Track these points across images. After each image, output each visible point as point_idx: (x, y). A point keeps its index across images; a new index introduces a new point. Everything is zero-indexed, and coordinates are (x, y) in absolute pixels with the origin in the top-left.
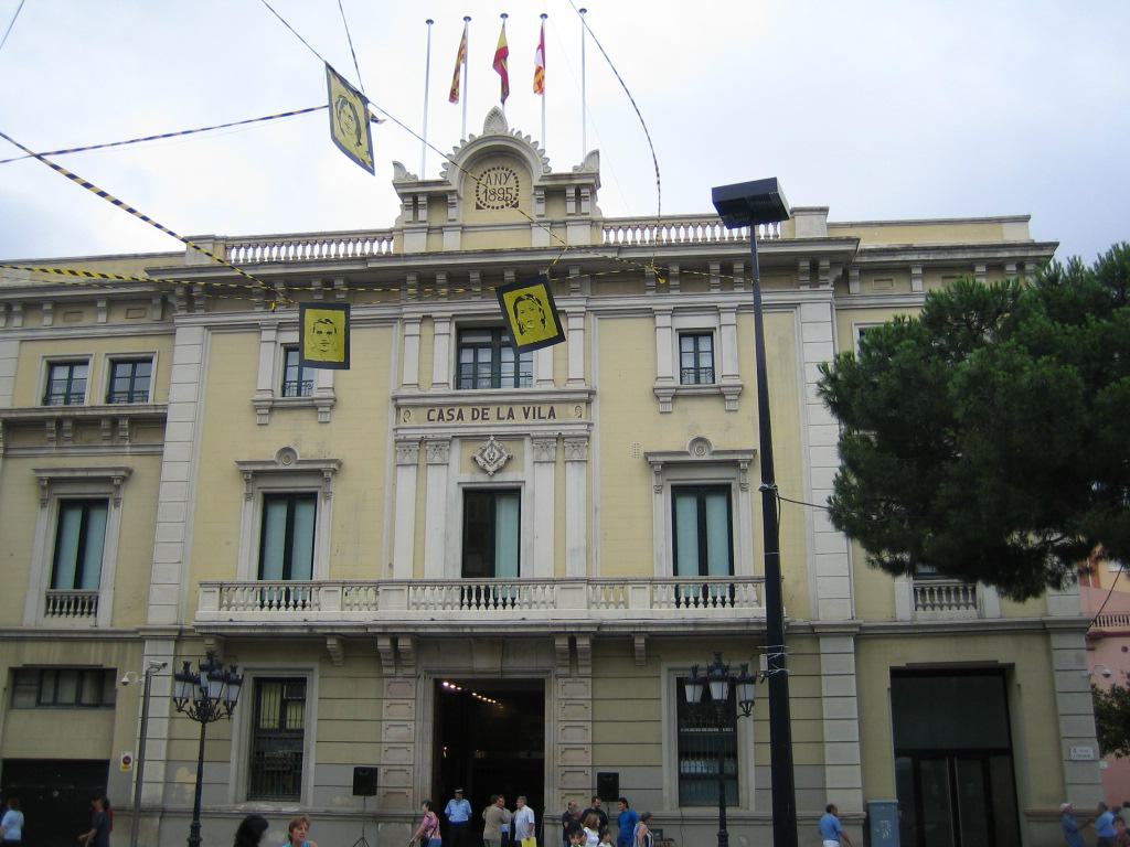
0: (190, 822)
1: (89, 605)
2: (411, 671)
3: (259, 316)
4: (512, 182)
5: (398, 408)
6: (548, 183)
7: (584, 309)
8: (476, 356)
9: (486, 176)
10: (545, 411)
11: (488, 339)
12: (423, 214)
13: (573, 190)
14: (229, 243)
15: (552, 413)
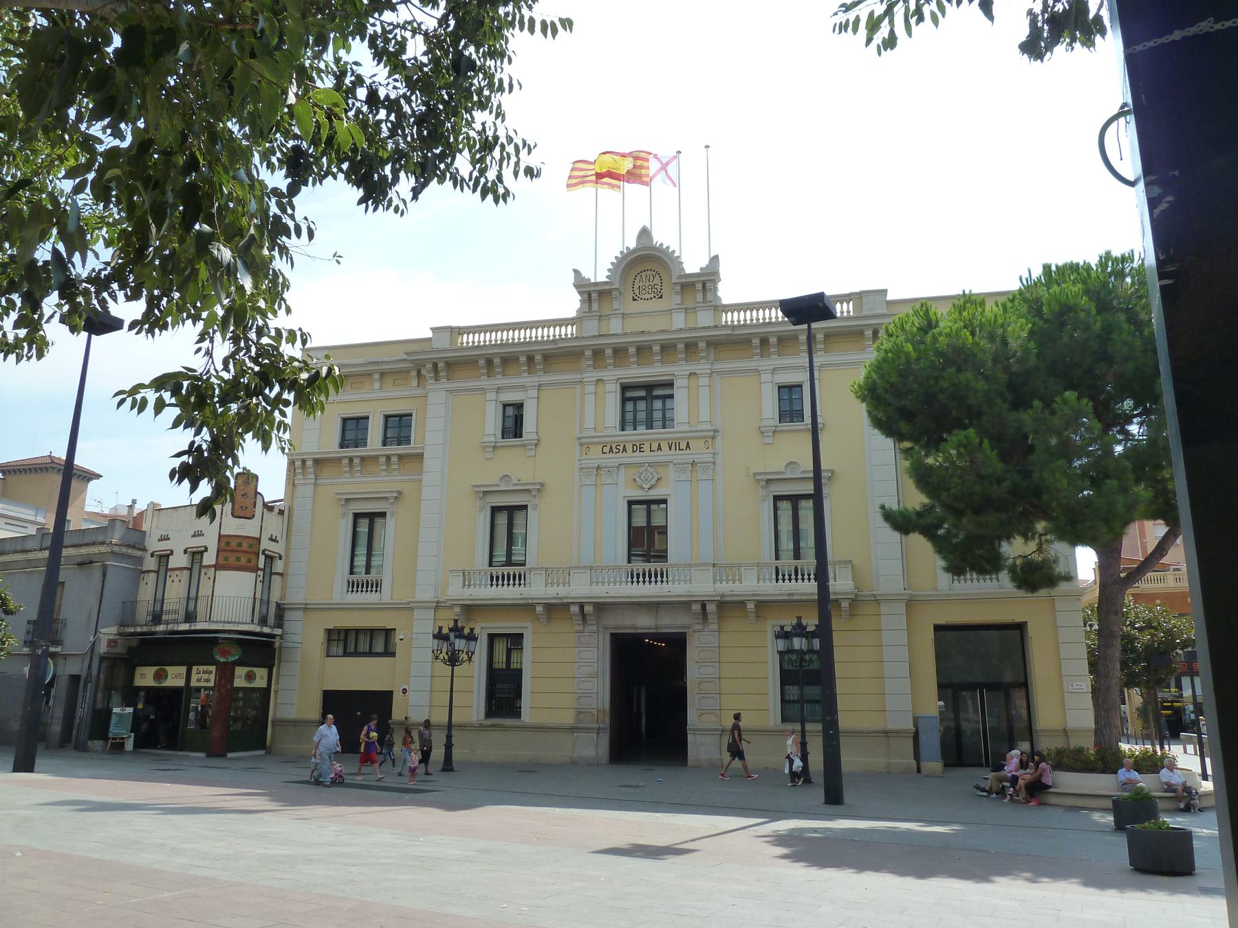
1: (376, 586)
2: (595, 628)
3: (484, 382)
5: (582, 445)
8: (635, 406)
10: (683, 446)
11: (642, 393)
12: (595, 306)
14: (461, 331)
15: (688, 446)
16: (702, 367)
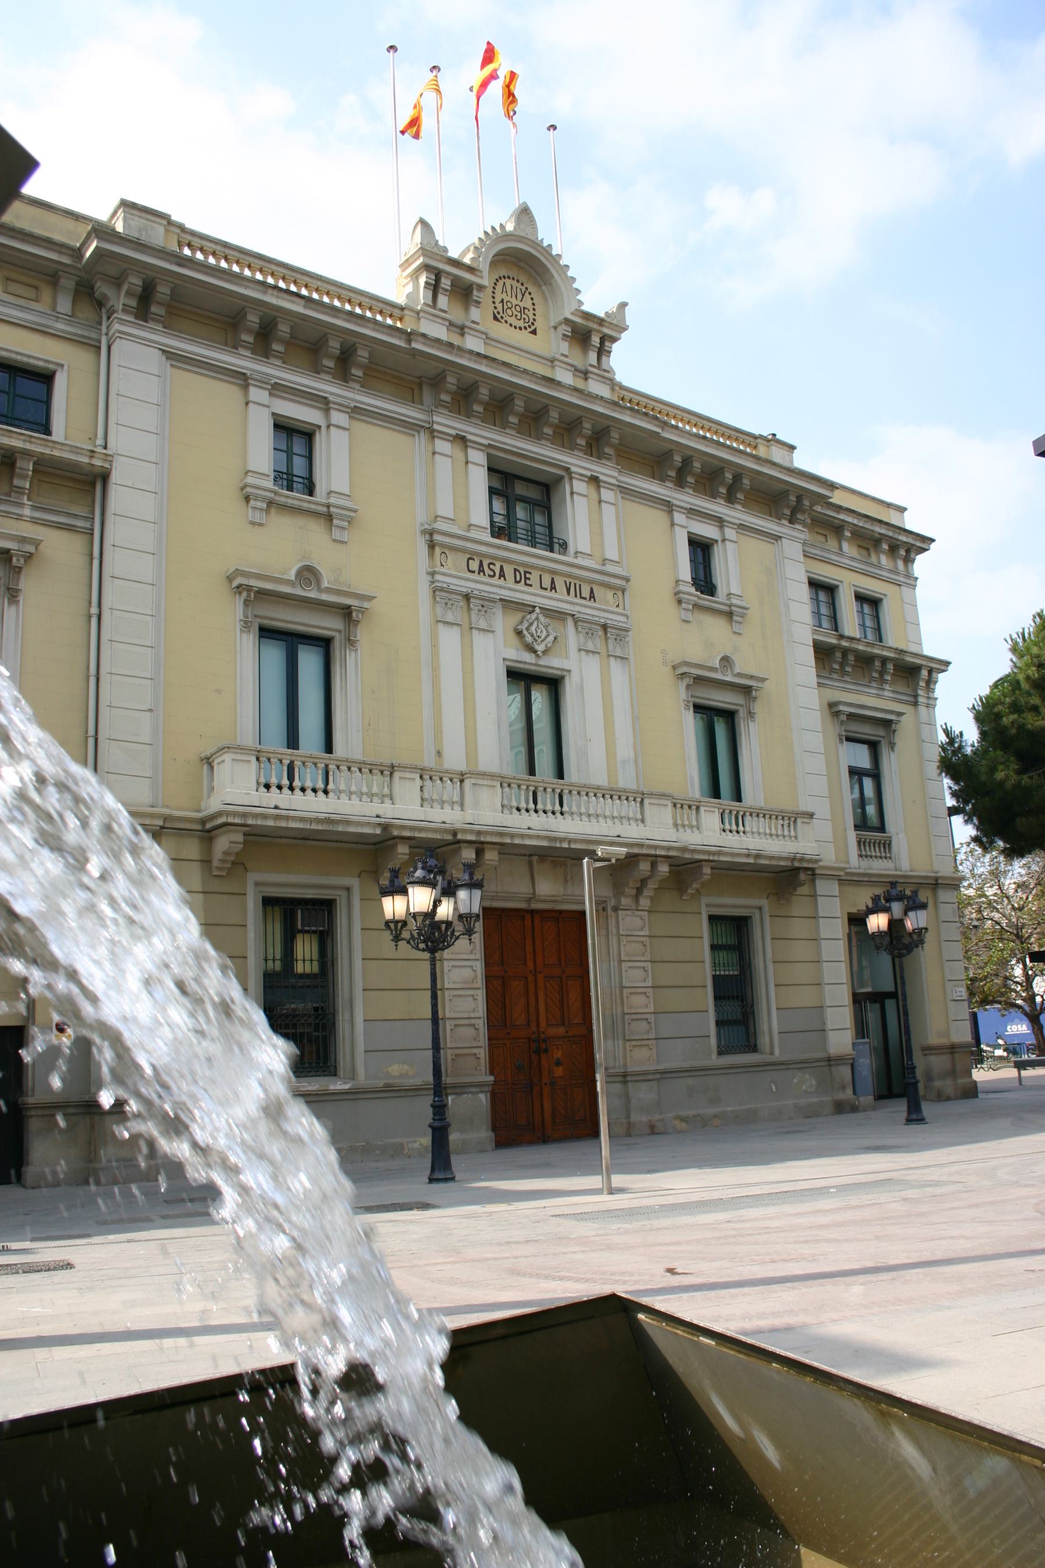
0: (430, 1100)
3: (243, 361)
4: (527, 303)
5: (432, 546)
6: (578, 320)
7: (614, 481)
9: (501, 283)
10: (586, 593)
13: (593, 335)
15: (592, 596)
16: (607, 471)
